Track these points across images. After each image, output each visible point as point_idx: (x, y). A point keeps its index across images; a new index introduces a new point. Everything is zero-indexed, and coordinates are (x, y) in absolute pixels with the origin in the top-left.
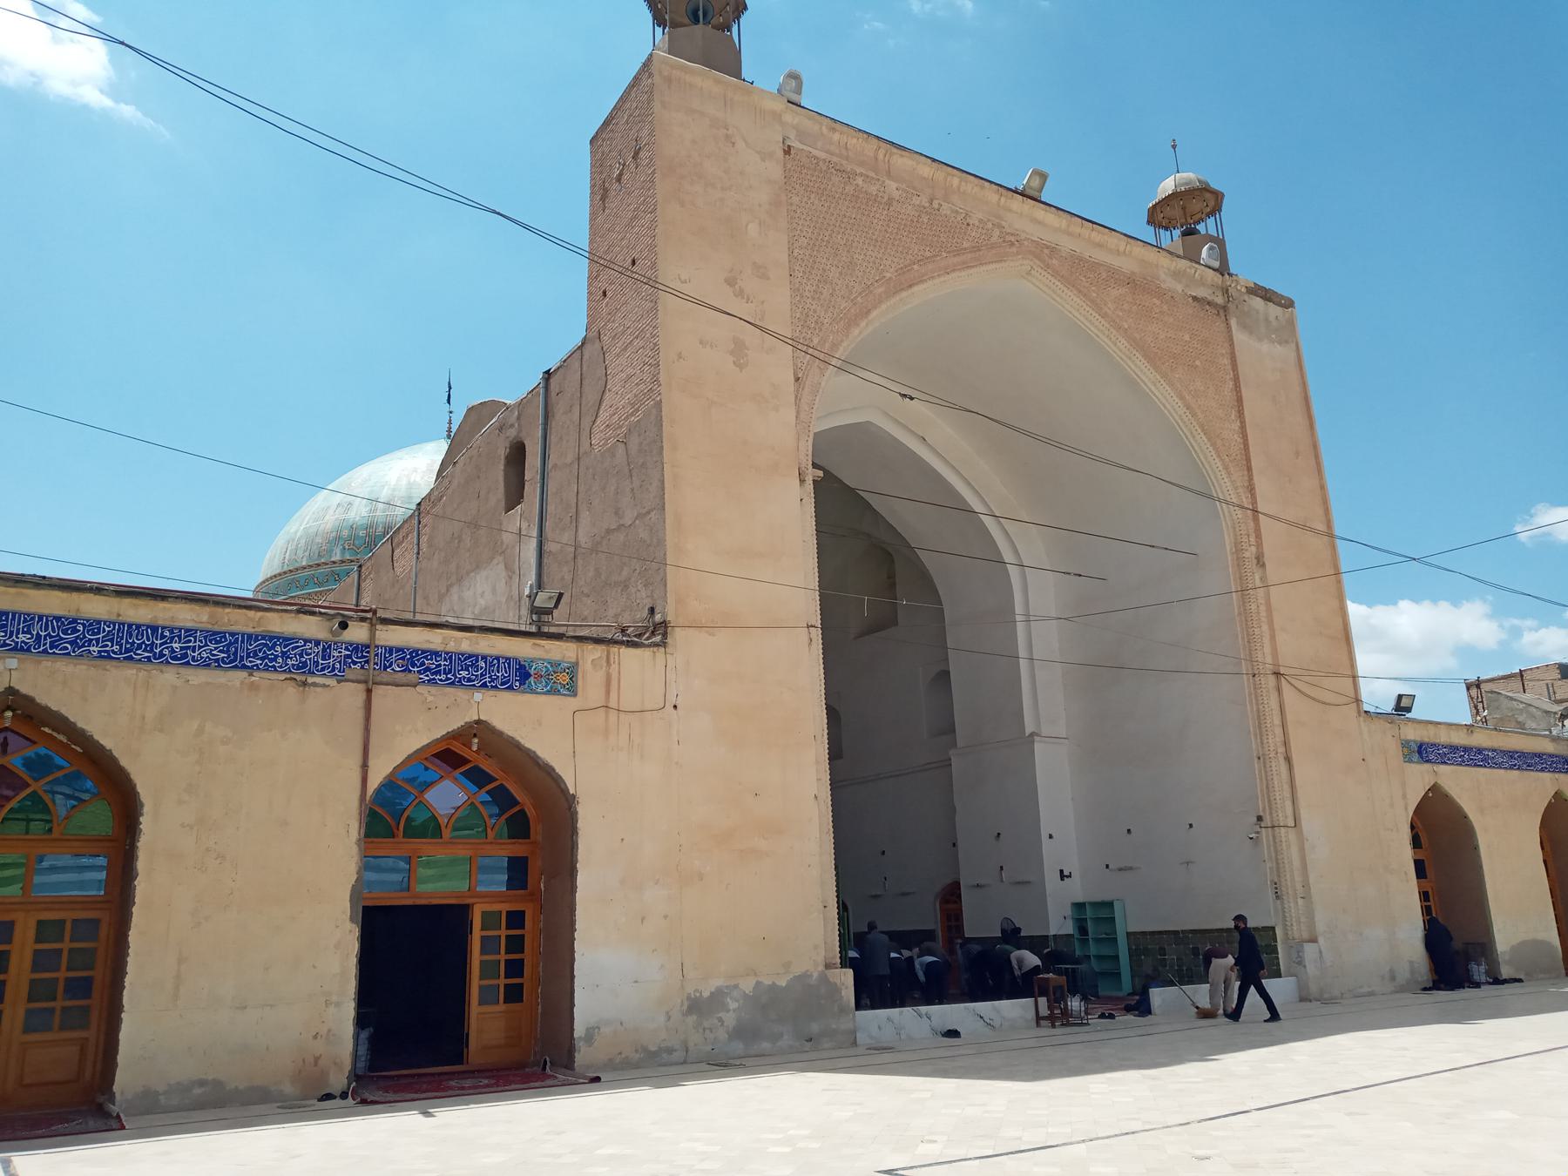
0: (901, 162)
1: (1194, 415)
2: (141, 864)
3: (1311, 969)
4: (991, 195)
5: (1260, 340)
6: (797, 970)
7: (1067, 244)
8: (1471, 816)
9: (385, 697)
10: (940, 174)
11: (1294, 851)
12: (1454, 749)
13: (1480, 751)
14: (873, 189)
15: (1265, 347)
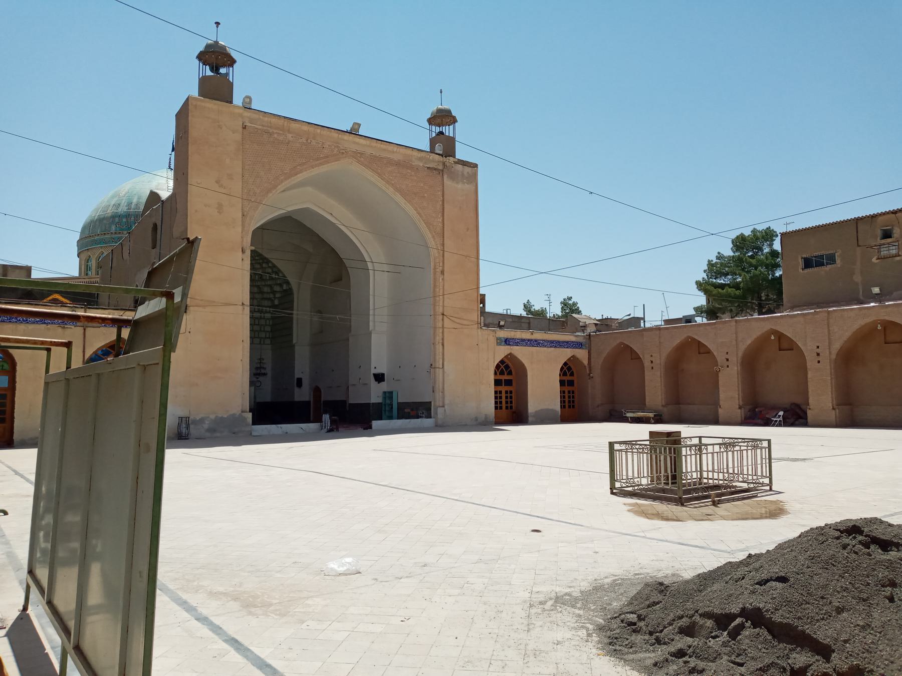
0: (294, 126)
1: (421, 216)
2: (17, 379)
3: (440, 416)
4: (335, 135)
5: (457, 183)
6: (232, 413)
7: (369, 151)
8: (526, 365)
9: (90, 331)
10: (311, 129)
11: (441, 375)
12: (523, 340)
13: (536, 341)
14: (281, 138)
15: (460, 186)
